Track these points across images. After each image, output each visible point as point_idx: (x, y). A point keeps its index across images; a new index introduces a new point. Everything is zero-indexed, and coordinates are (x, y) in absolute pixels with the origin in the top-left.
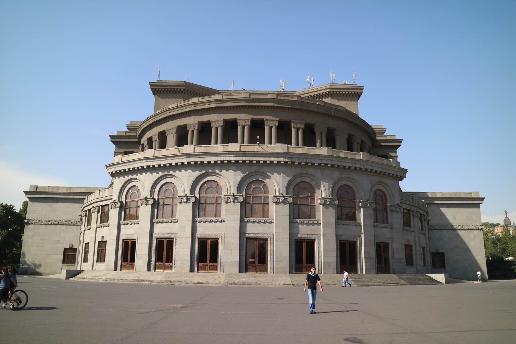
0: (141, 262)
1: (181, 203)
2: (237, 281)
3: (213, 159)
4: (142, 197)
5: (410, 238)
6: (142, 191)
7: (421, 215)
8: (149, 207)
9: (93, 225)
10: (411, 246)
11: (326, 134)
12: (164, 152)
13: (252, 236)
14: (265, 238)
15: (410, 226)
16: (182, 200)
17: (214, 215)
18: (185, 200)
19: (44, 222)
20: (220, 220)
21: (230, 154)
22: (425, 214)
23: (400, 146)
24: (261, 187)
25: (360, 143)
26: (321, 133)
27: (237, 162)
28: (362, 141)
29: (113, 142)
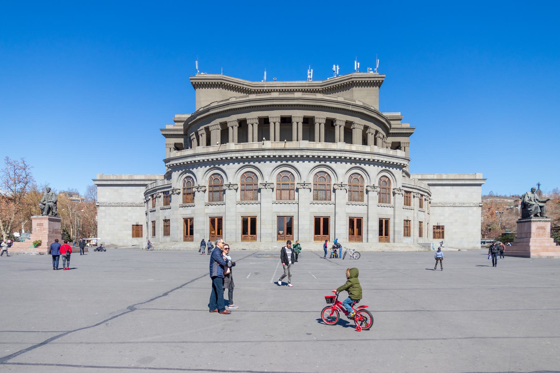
0: (198, 235)
2: (270, 248)
3: (250, 154)
5: (408, 214)
7: (422, 195)
9: (157, 208)
10: (410, 221)
11: (345, 128)
12: (211, 149)
13: (281, 214)
15: (410, 205)
19: (113, 205)
22: (426, 194)
23: (411, 133)
25: (374, 133)
26: (340, 126)
28: (377, 132)
29: (163, 135)
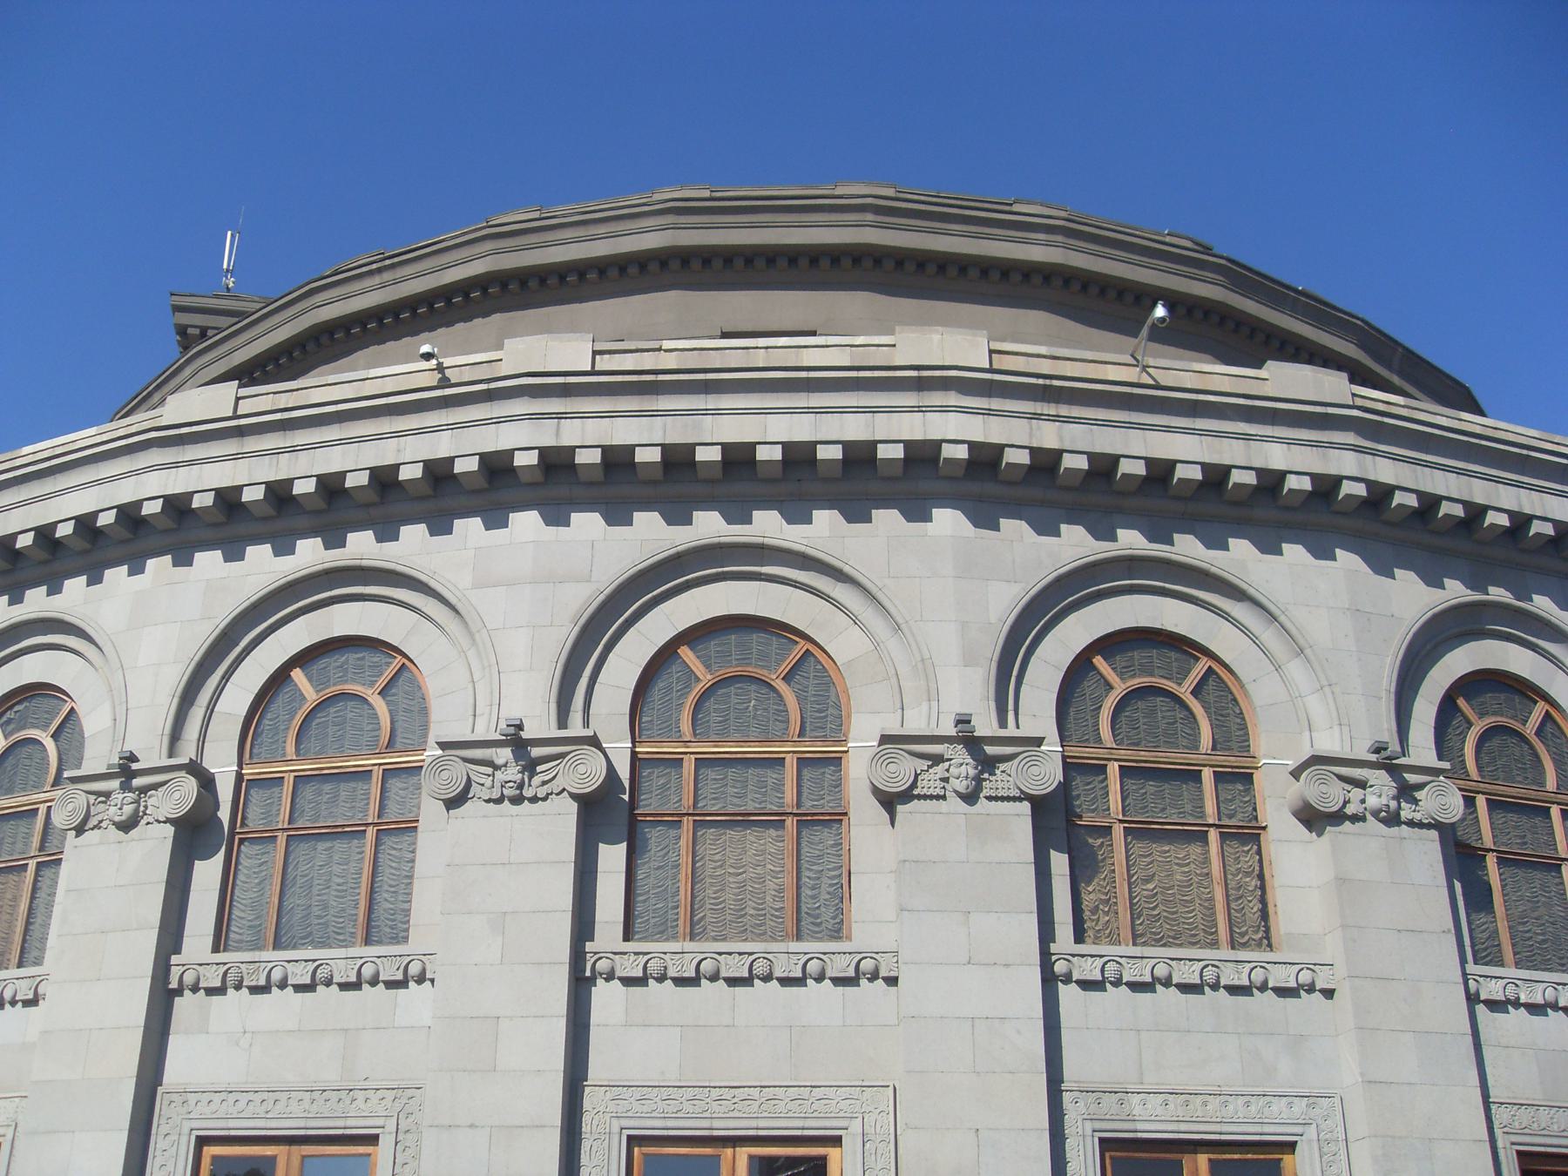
1: (453, 803)
4: (98, 757)
6: (95, 722)
8: (156, 842)
14: (1272, 1133)
16: (479, 774)
17: (790, 924)
18: (513, 773)
20: (841, 966)
21: (924, 381)
24: (1184, 690)
27: (985, 458)
